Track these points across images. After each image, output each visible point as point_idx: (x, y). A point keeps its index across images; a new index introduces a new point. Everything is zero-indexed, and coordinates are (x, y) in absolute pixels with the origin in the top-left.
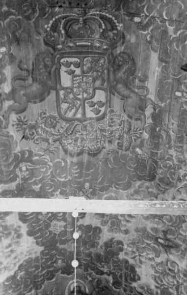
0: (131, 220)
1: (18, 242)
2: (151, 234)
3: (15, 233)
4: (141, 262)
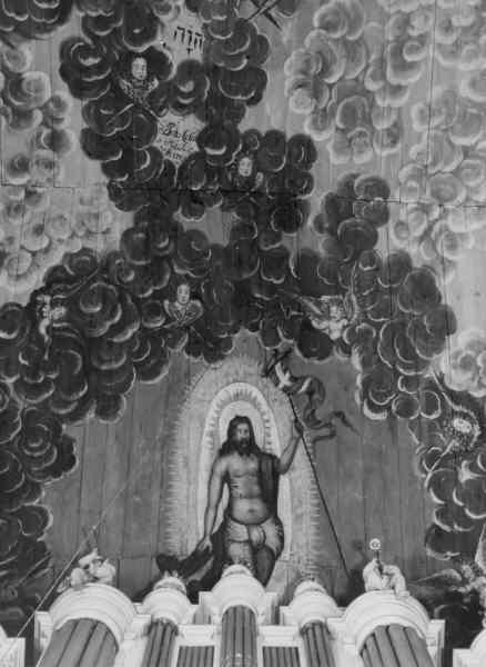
0: (403, 83)
1: (50, 165)
2: (475, 105)
3: (44, 123)
4: (453, 242)
